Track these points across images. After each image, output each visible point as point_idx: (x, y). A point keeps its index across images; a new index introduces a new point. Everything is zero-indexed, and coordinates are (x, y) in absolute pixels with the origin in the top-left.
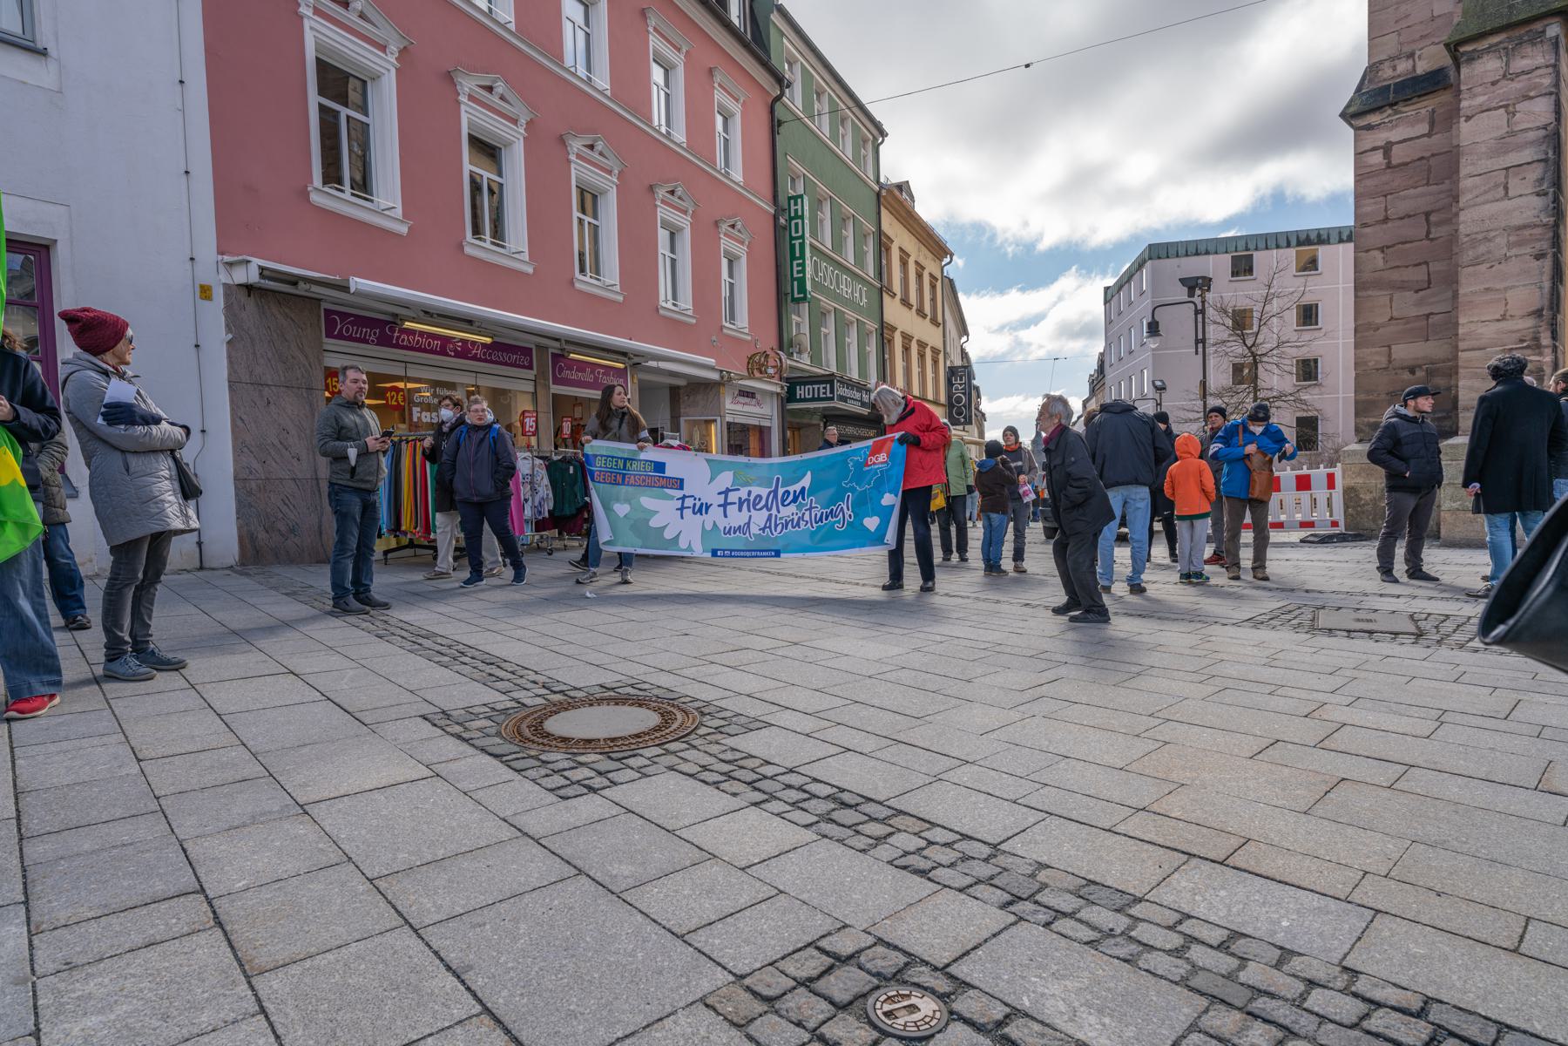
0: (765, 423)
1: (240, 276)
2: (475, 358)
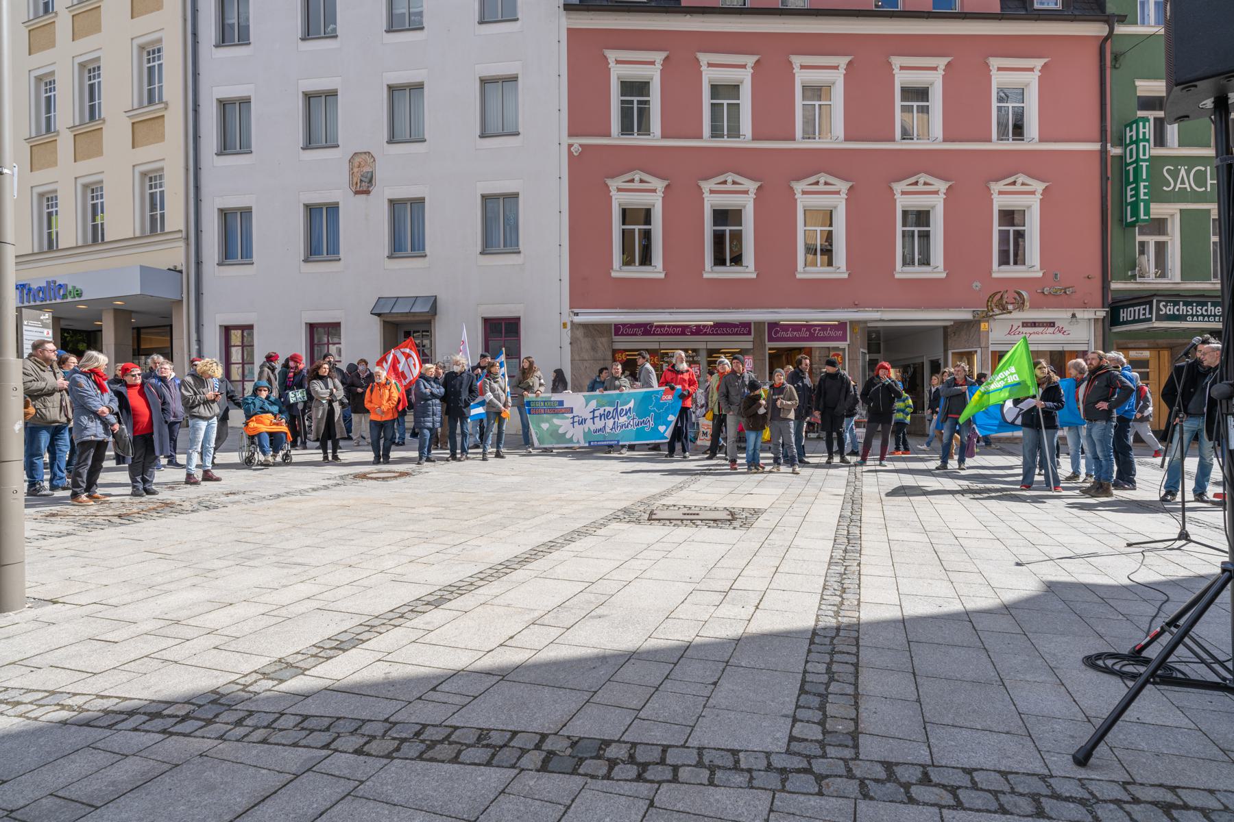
2: (705, 334)
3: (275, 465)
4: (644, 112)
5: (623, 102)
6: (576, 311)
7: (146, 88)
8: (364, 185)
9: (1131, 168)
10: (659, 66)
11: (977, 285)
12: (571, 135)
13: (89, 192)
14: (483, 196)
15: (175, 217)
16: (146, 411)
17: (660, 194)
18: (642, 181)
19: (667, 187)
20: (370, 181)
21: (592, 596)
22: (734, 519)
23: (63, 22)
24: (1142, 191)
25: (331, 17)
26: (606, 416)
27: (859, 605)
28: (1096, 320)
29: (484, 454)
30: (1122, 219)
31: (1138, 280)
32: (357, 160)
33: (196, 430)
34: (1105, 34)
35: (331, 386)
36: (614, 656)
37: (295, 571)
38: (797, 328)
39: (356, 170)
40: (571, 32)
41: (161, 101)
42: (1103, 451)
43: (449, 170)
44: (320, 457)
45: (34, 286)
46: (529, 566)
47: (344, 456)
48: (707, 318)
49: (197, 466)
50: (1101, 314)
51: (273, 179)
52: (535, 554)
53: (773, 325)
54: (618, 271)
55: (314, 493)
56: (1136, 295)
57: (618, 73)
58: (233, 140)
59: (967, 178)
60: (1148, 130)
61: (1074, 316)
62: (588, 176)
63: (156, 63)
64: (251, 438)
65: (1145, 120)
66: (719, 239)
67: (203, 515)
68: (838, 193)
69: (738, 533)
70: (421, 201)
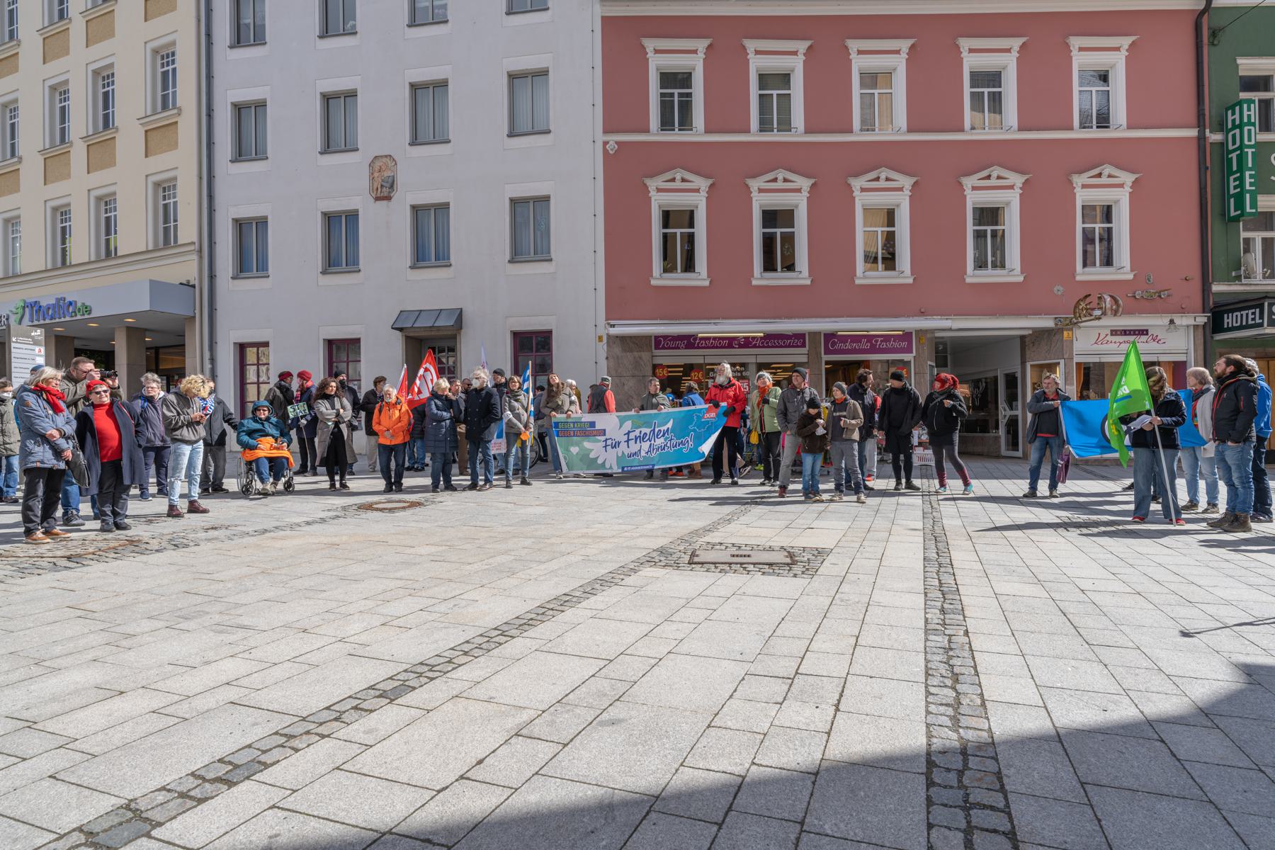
0: (1182, 358)
1: (613, 331)
2: (755, 346)
3: (273, 494)
4: (686, 106)
5: (662, 95)
6: (612, 322)
7: (159, 94)
8: (384, 191)
9: (1234, 156)
10: (701, 55)
11: (1058, 289)
12: (606, 131)
13: (103, 204)
14: (512, 200)
15: (188, 229)
16: (116, 434)
17: (704, 194)
18: (683, 180)
19: (712, 186)
20: (392, 187)
21: (606, 683)
22: (794, 563)
23: (77, 28)
24: (1248, 180)
25: (349, 12)
26: (641, 438)
27: (983, 704)
28: (1196, 327)
29: (508, 481)
30: (1224, 213)
31: (1244, 281)
32: (378, 164)
33: (178, 456)
34: (1202, 7)
35: (338, 405)
36: (625, 804)
37: (232, 638)
38: (857, 339)
39: (376, 175)
40: (606, 20)
41: (174, 106)
42: (1240, 478)
43: (475, 173)
44: (327, 485)
45: (44, 303)
46: (532, 633)
47: (354, 484)
48: (755, 328)
49: (182, 496)
50: (1202, 319)
51: (290, 187)
52: (544, 612)
53: (830, 336)
54: (658, 278)
55: (308, 528)
56: (1242, 298)
57: (656, 64)
58: (248, 146)
59: (1047, 173)
60: (1252, 113)
61: (1172, 322)
62: (624, 175)
63: (170, 68)
64: (249, 463)
65: (1250, 101)
66: (768, 242)
67: (170, 555)
68: (901, 189)
69: (801, 582)
70: (446, 206)
